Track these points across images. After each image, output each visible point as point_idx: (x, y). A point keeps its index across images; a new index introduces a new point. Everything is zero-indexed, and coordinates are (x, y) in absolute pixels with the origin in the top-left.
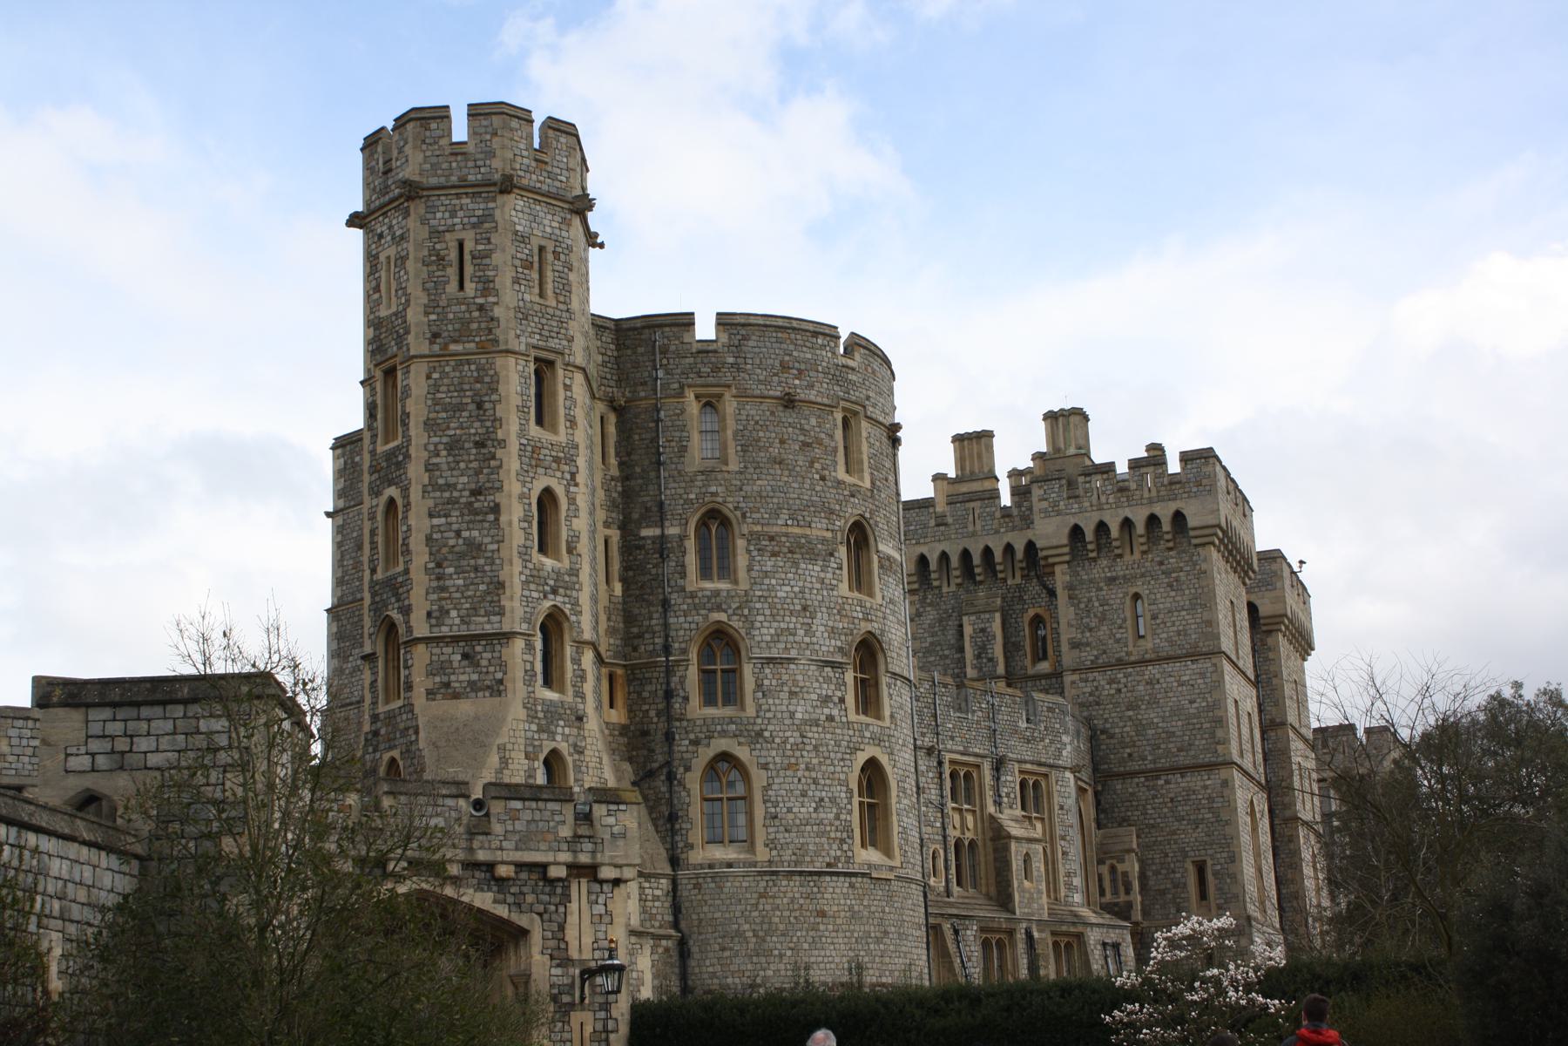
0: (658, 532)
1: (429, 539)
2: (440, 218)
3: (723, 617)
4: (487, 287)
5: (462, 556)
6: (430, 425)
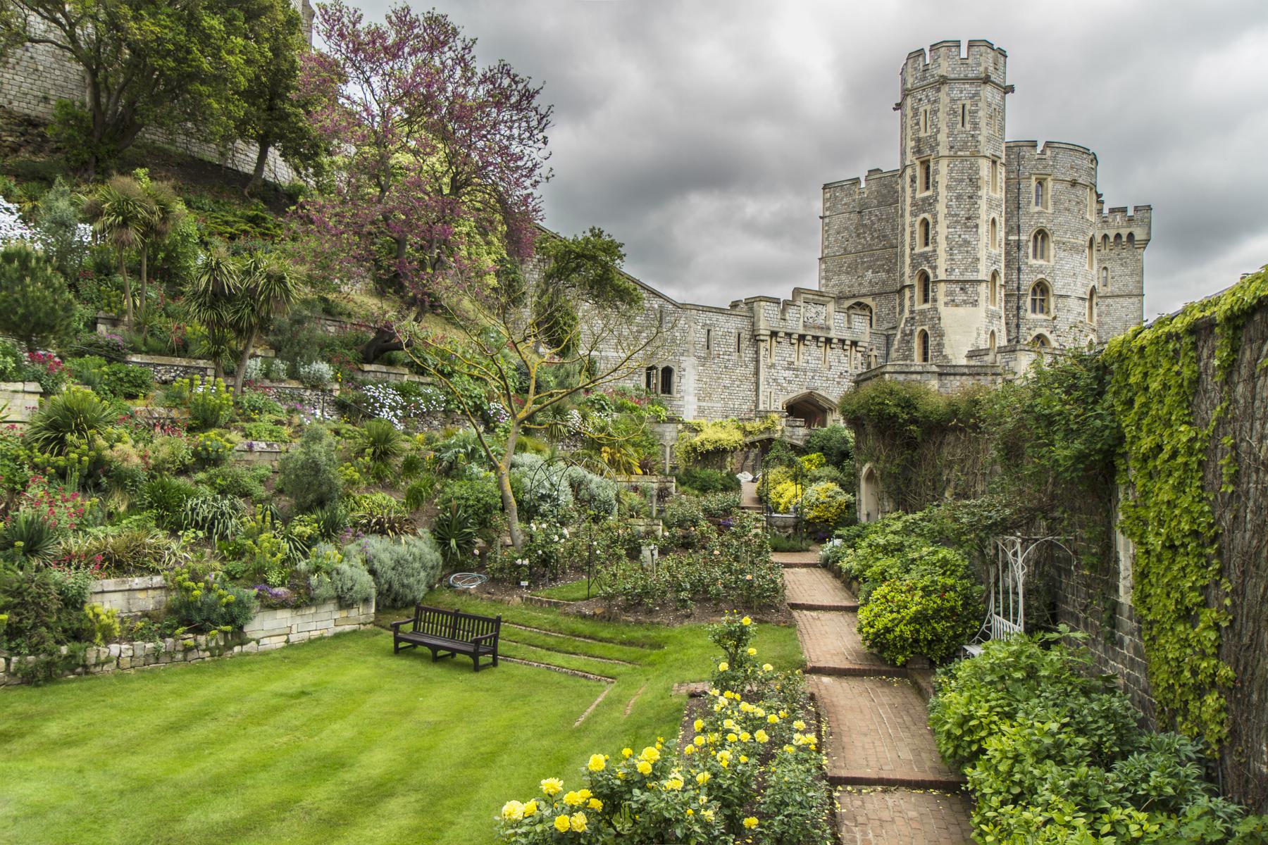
0: (1017, 238)
1: (947, 237)
2: (955, 94)
3: (1043, 276)
4: (975, 126)
5: (961, 246)
6: (949, 187)
